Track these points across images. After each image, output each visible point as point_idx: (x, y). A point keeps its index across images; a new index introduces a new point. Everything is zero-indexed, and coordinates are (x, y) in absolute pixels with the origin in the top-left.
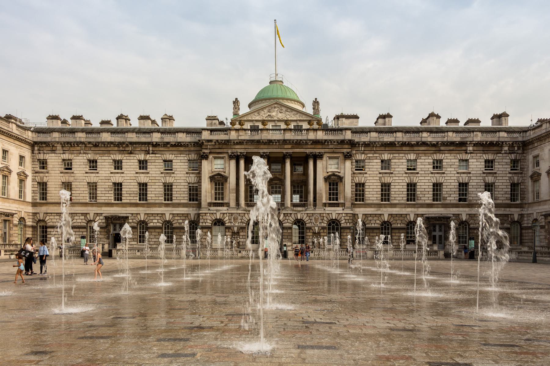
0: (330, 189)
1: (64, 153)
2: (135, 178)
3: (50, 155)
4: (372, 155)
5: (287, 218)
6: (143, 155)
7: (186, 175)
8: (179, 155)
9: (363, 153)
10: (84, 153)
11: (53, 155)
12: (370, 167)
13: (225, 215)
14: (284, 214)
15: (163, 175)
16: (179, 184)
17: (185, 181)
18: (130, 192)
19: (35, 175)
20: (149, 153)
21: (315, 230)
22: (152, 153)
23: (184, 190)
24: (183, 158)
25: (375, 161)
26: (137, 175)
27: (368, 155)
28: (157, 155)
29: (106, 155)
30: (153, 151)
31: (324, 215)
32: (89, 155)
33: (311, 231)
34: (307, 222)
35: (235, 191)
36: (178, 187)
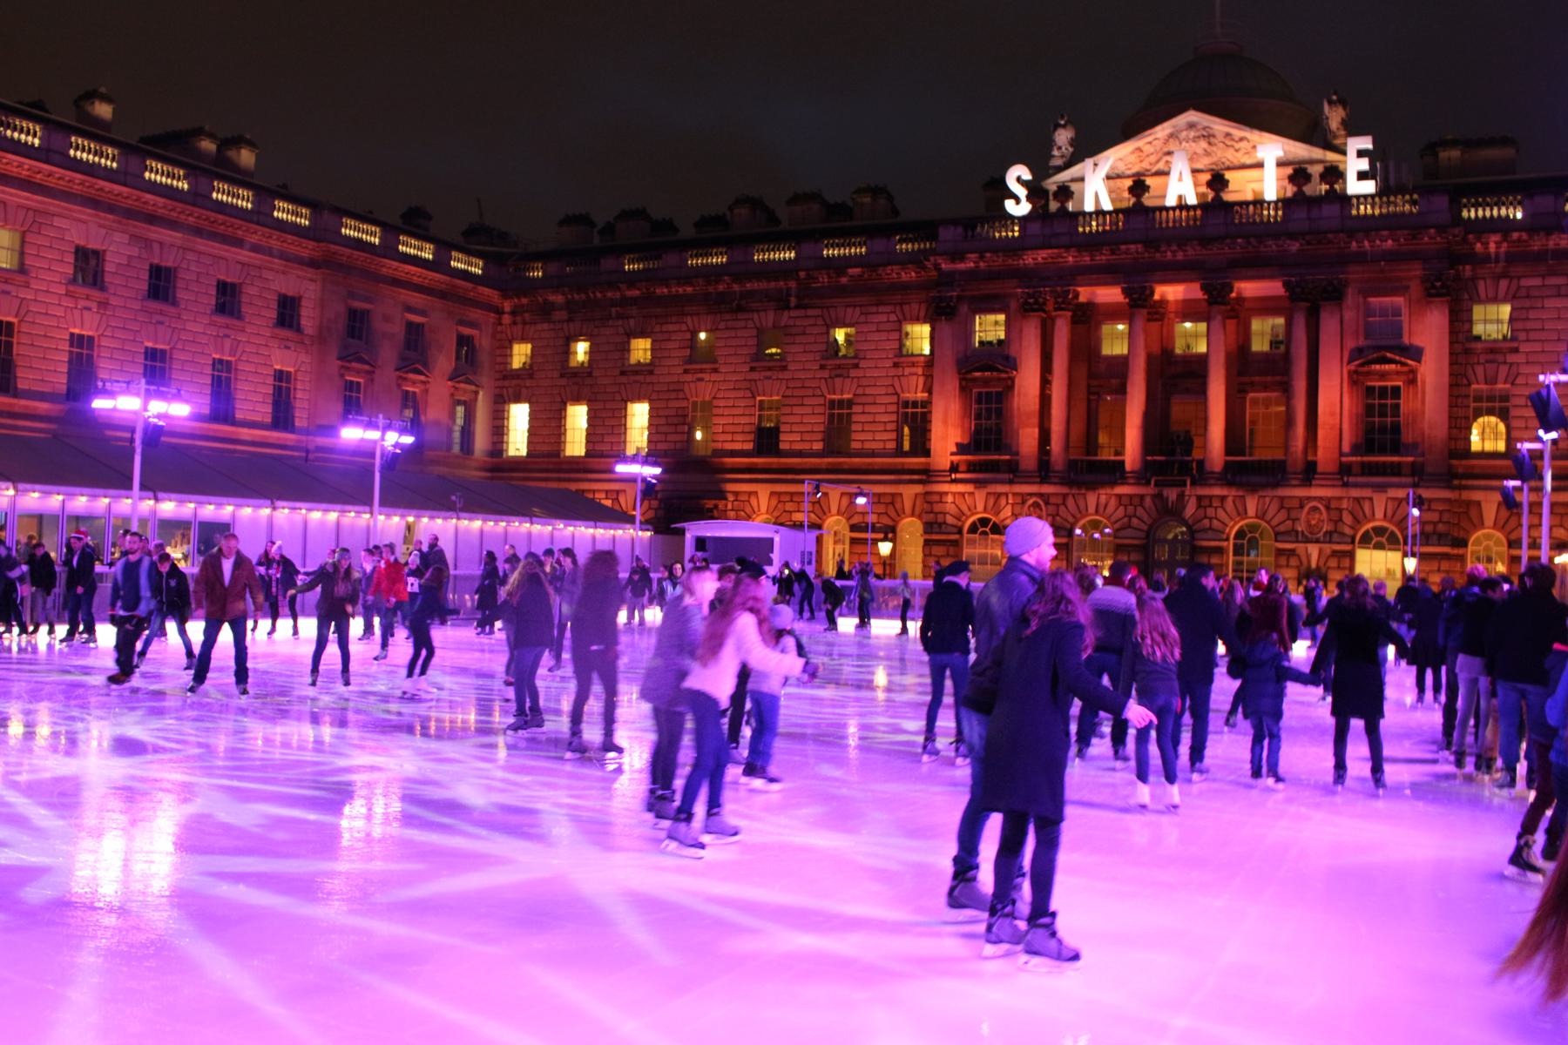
0: (1369, 410)
1: (570, 320)
2: (747, 384)
3: (539, 327)
4: (1537, 282)
5: (1210, 512)
6: (771, 315)
7: (892, 372)
8: (874, 309)
9: (1504, 275)
10: (620, 316)
11: (546, 326)
12: (1529, 325)
13: (1003, 501)
14: (1200, 498)
15: (826, 374)
16: (870, 400)
17: (891, 390)
18: (731, 428)
19: (500, 383)
20: (788, 308)
21: (1308, 557)
22: (798, 307)
23: (885, 418)
24: (884, 318)
25: (1549, 303)
26: (755, 375)
27: (1524, 282)
28: (810, 312)
29: (674, 319)
30: (797, 297)
31: (1345, 504)
32: (632, 322)
33: (1293, 562)
34: (1282, 528)
35: (1035, 420)
36: (868, 409)
